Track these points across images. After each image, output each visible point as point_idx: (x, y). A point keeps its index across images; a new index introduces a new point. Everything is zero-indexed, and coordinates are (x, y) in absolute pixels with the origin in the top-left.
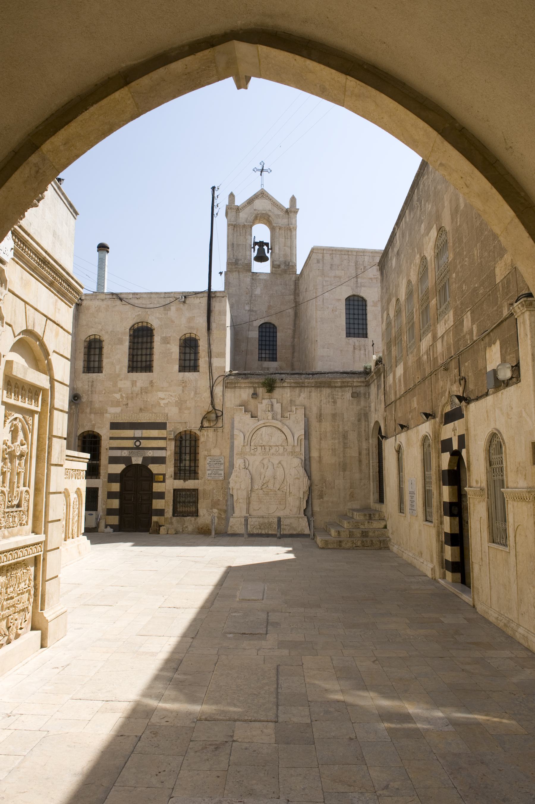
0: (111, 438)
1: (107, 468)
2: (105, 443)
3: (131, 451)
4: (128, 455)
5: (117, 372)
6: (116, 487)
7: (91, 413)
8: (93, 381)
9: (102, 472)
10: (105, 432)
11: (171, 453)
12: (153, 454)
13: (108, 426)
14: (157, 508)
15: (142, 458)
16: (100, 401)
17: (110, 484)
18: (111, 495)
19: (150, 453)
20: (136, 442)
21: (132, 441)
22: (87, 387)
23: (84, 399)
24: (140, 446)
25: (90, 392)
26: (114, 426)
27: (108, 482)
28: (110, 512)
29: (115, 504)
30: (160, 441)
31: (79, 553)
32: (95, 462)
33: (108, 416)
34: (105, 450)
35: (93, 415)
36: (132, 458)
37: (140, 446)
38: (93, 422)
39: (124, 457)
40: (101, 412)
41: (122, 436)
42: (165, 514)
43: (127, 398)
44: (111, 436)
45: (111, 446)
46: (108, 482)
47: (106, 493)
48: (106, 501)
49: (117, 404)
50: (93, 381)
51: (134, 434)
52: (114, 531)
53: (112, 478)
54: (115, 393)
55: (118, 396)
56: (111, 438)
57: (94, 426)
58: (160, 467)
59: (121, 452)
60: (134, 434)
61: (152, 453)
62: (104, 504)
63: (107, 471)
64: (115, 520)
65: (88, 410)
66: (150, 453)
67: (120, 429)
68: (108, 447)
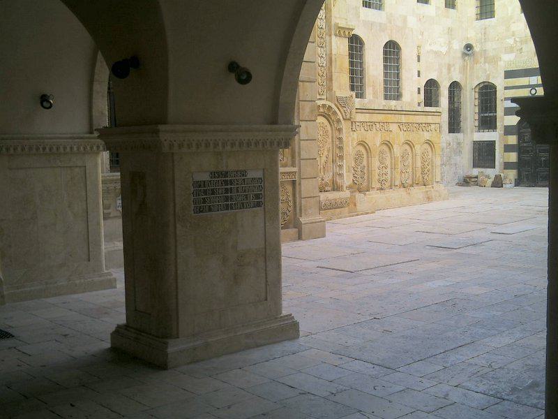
0: (506, 88)
1: (503, 120)
2: (501, 94)
5: (510, 15)
6: (513, 140)
7: (485, 62)
8: (485, 28)
9: (498, 124)
10: (499, 82)
13: (503, 75)
16: (494, 49)
18: (508, 148)
22: (480, 35)
23: (477, 49)
25: (483, 41)
26: (509, 74)
28: (507, 166)
29: (513, 157)
31: (428, 198)
32: (491, 114)
33: (501, 64)
34: (500, 102)
35: (487, 64)
38: (488, 72)
40: (494, 60)
41: (517, 84)
43: (521, 41)
44: (507, 86)
47: (503, 146)
49: (510, 50)
50: (485, 28)
53: (508, 130)
54: (509, 38)
55: (511, 41)
56: (506, 88)
57: (489, 76)
63: (503, 123)
64: (512, 174)
65: (482, 60)
68: (503, 98)
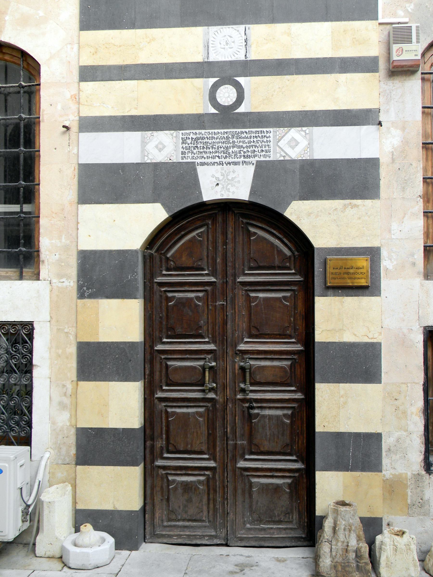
3: (192, 134)
4: (177, 158)
11: (405, 142)
12: (310, 145)
14: (342, 429)
15: (251, 170)
17: (89, 302)
19: (294, 143)
20: (215, 88)
21: (199, 82)
24: (242, 109)
27: (81, 296)
30: (343, 77)
36: (200, 170)
37: (242, 109)
39: (156, 166)
42: (385, 461)
45: (87, 112)
46: (81, 296)
47: (73, 350)
48: (75, 394)
51: (207, 47)
52: (119, 546)
58: (350, 212)
59: (144, 144)
60: (207, 47)
61: (303, 143)
62: (62, 406)
66: (294, 143)
67: (133, 26)
